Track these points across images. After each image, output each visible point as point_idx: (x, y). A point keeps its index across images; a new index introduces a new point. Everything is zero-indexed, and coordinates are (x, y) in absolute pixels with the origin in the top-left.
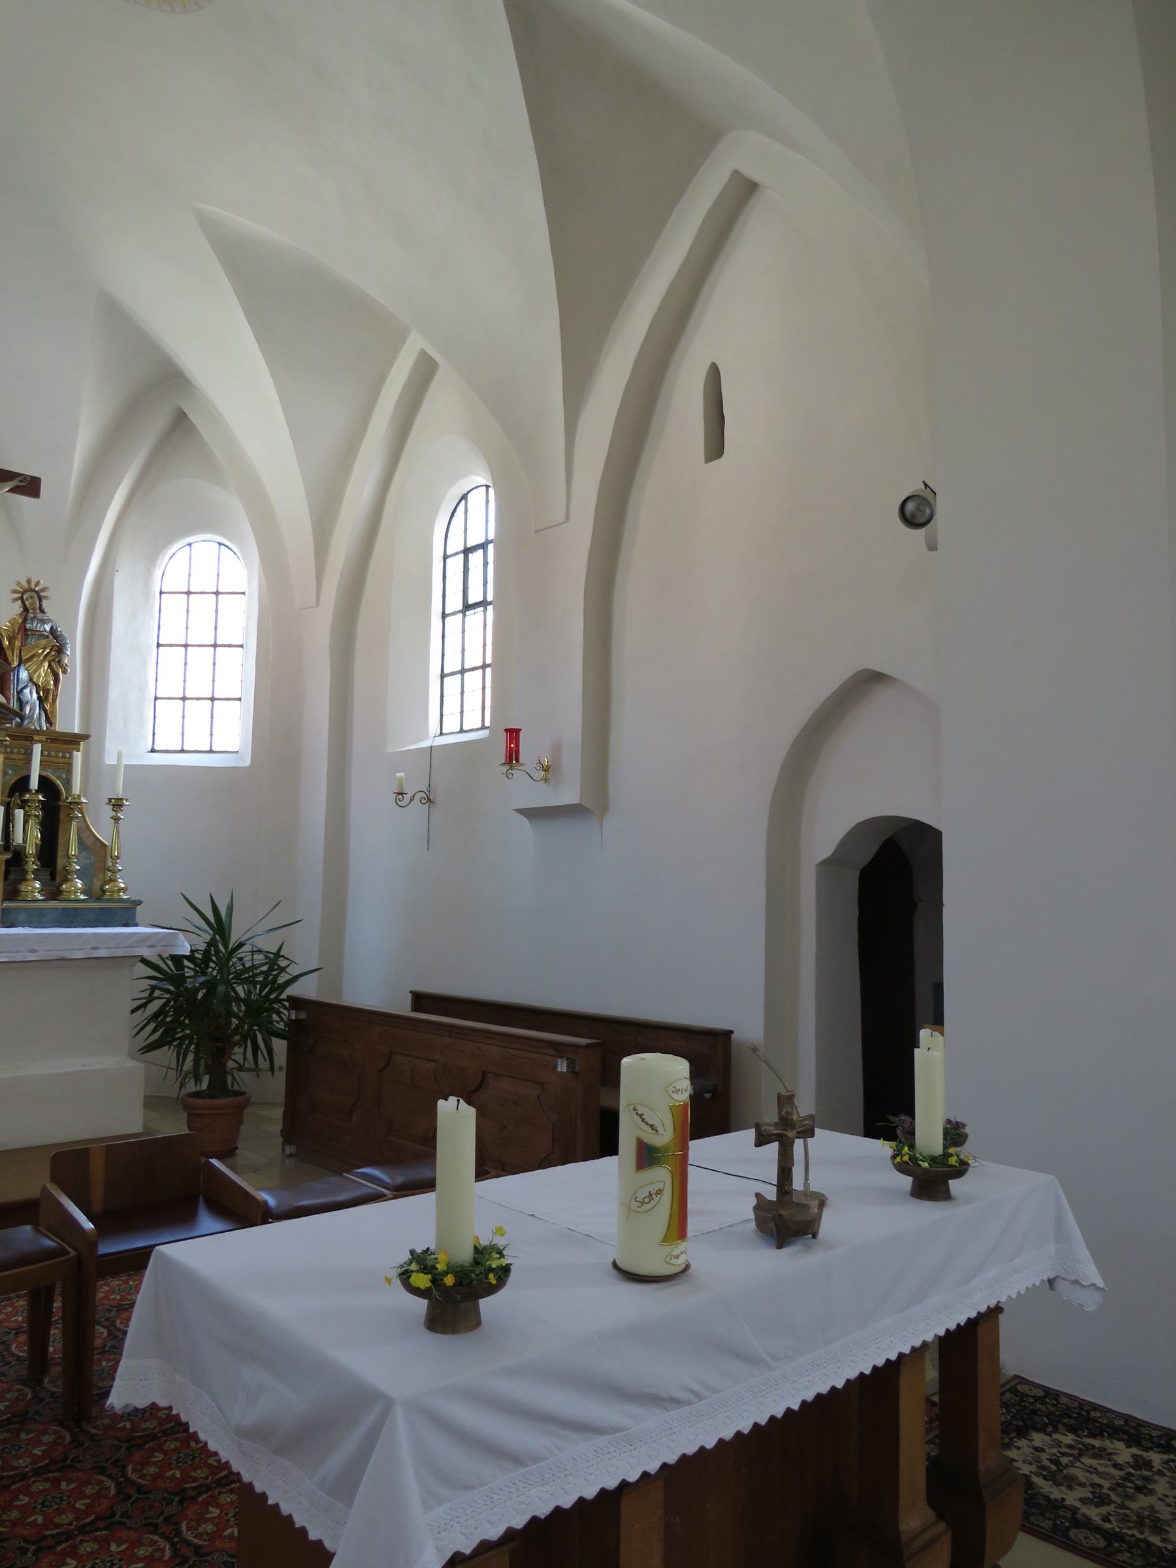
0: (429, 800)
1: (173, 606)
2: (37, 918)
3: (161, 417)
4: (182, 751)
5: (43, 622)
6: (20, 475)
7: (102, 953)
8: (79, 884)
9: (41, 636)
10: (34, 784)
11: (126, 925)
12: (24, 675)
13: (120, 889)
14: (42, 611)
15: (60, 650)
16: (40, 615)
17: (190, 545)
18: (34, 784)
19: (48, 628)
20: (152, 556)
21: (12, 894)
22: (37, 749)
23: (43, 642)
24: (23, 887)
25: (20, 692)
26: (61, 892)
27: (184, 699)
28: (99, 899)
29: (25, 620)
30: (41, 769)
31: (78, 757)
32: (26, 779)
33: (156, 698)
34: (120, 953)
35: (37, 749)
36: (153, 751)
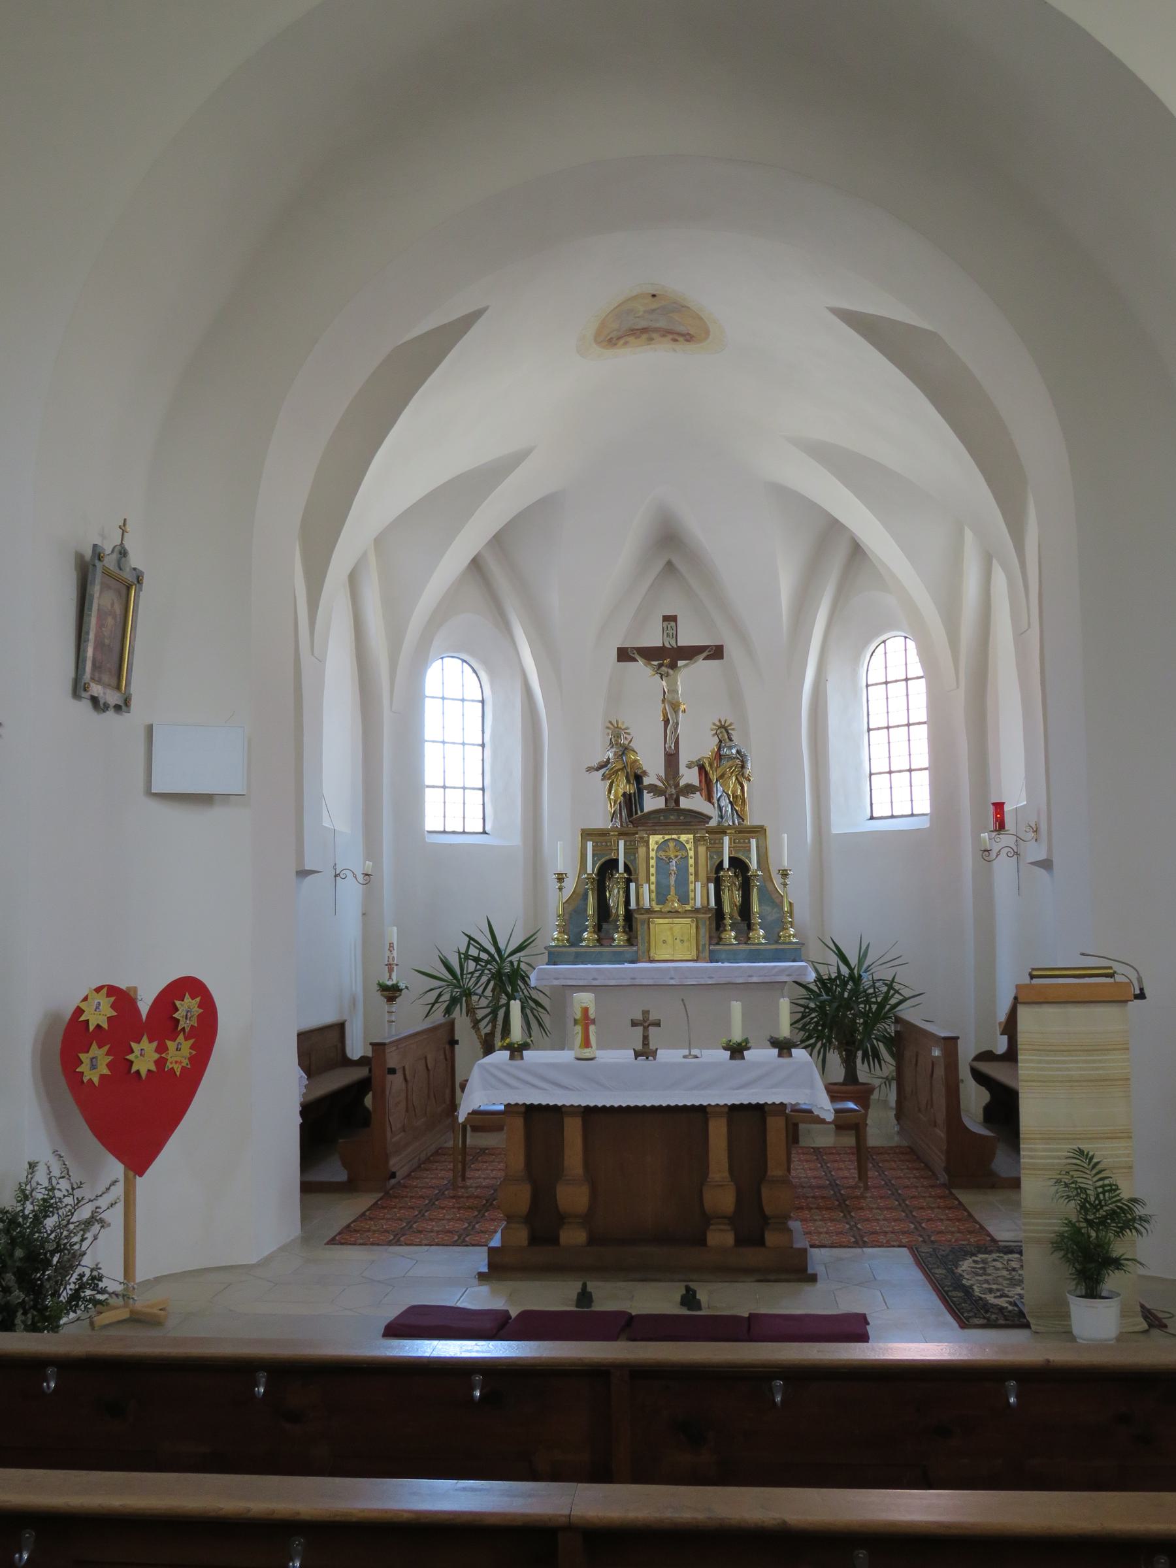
0: (1017, 854)
1: (877, 693)
2: (734, 957)
3: (837, 557)
4: (892, 817)
5: (730, 748)
6: (708, 646)
7: (755, 979)
8: (761, 932)
9: (731, 758)
10: (726, 865)
11: (794, 961)
12: (720, 788)
13: (790, 936)
14: (731, 740)
15: (743, 767)
16: (729, 744)
17: (884, 642)
18: (726, 865)
19: (734, 751)
20: (855, 659)
21: (719, 940)
22: (726, 839)
23: (730, 763)
24: (723, 936)
25: (718, 800)
26: (749, 938)
27: (890, 772)
28: (777, 942)
29: (719, 749)
30: (730, 852)
31: (753, 842)
32: (721, 863)
33: (871, 774)
34: (767, 979)
35: (726, 839)
36: (872, 818)
